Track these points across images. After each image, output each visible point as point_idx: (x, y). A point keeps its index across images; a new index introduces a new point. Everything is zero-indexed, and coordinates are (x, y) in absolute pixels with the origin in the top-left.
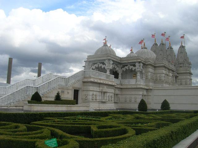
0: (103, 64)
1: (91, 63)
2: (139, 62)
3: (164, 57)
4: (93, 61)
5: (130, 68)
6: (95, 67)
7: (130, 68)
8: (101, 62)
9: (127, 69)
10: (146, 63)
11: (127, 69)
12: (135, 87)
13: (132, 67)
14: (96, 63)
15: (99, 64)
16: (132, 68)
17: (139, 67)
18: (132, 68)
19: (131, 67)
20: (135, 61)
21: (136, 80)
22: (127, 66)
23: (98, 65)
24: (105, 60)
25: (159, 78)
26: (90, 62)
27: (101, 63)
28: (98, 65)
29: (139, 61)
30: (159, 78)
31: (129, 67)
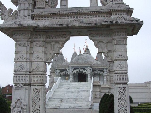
0: (84, 69)
1: (73, 69)
2: (106, 69)
4: (75, 67)
5: (98, 73)
7: (98, 73)
8: (82, 68)
10: (111, 70)
12: (105, 87)
13: (100, 72)
14: (78, 69)
15: (80, 69)
16: (99, 73)
17: (105, 73)
18: (99, 73)
19: (99, 72)
20: (103, 68)
21: (104, 82)
22: (95, 71)
23: (80, 70)
24: (87, 67)
25: (112, 80)
26: (72, 67)
27: (82, 69)
28: (80, 70)
29: (106, 68)
31: (97, 72)
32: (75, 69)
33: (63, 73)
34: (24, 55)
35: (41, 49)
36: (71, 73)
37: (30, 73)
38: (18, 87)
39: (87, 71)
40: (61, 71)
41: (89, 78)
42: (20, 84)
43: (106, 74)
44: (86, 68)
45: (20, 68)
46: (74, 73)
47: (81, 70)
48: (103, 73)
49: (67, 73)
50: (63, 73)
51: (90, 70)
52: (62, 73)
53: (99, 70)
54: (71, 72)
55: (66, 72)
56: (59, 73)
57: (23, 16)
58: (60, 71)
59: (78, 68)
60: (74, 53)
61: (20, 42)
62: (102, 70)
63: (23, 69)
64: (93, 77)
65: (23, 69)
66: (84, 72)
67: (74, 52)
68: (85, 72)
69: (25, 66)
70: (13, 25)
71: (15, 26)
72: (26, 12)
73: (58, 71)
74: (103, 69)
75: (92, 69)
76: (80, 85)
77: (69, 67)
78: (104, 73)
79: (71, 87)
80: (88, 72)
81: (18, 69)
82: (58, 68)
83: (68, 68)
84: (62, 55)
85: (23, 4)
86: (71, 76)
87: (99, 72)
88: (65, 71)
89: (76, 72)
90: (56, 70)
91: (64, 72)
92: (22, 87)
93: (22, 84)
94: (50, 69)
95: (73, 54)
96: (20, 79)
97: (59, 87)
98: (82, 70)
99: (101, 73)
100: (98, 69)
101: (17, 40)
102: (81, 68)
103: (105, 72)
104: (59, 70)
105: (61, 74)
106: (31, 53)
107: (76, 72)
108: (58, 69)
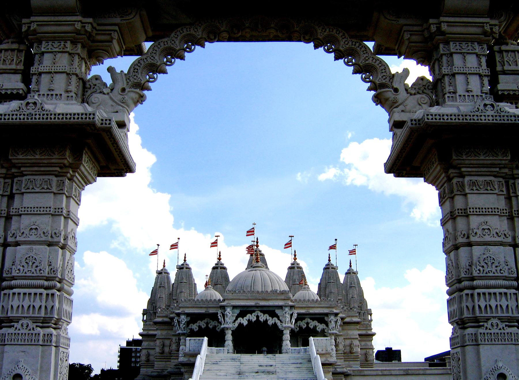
0: (273, 314)
1: (237, 311)
2: (336, 315)
3: (340, 298)
5: (312, 327)
6: (249, 321)
7: (312, 327)
8: (265, 309)
9: (304, 327)
11: (304, 327)
13: (315, 323)
14: (251, 312)
15: (260, 314)
19: (313, 324)
20: (326, 311)
23: (258, 317)
24: (281, 307)
26: (234, 307)
27: (264, 312)
28: (258, 317)
29: (335, 311)
30: (348, 349)
31: (308, 324)
32: (242, 314)
33: (200, 327)
36: (231, 325)
38: (488, 331)
39: (281, 322)
40: (194, 318)
41: (287, 343)
42: (495, 321)
43: (335, 331)
44: (278, 312)
45: (485, 266)
46: (241, 325)
47: (263, 317)
48: (327, 325)
49: (211, 327)
50: (200, 327)
51: (292, 315)
52: (195, 327)
53: (313, 319)
54: (230, 322)
55: (207, 324)
56: (188, 324)
57: (466, 94)
58: (189, 319)
59: (254, 311)
60: (216, 264)
61: (474, 178)
62: (321, 318)
63: (498, 269)
64: (311, 339)
65: (498, 269)
66: (271, 321)
67: (216, 261)
68: (273, 322)
69: (502, 260)
70: (476, 118)
71: (483, 120)
72: (475, 83)
73: (184, 319)
74: (327, 315)
75: (295, 316)
77: (223, 308)
78: (330, 327)
79: (244, 368)
80: (287, 323)
81: (481, 269)
82: (184, 309)
83: (219, 312)
84: (187, 268)
85: (460, 56)
86: (229, 337)
87: (313, 324)
88: (206, 321)
89: (245, 323)
90: (178, 315)
91: (202, 324)
92: (502, 331)
93: (500, 318)
94: (144, 314)
95: (214, 268)
96: (493, 303)
97: (207, 368)
98: (266, 317)
99: (320, 327)
101: (463, 169)
102: (261, 311)
103: (332, 325)
104: (188, 315)
105: (192, 330)
107: (245, 323)
108: (185, 314)
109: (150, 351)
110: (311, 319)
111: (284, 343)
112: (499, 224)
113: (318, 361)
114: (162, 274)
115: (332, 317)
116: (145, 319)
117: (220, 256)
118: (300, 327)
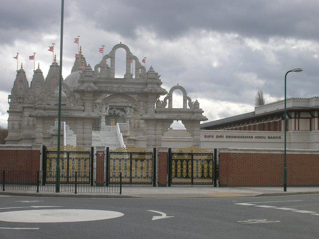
2: (131, 107)
19: (117, 112)
30: (137, 125)
31: (114, 111)
34: (152, 131)
35: (160, 128)
37: (155, 140)
51: (106, 108)
64: (118, 124)
74: (126, 107)
75: (108, 108)
76: (98, 135)
87: (117, 112)
94: (9, 98)
99: (121, 113)
100: (117, 106)
106: (155, 130)
109: (14, 122)
110: (117, 109)
111: (102, 123)
112: (153, 132)
113: (121, 136)
114: (21, 73)
115: (128, 109)
116: (10, 101)
117: (55, 58)
118: (110, 113)
